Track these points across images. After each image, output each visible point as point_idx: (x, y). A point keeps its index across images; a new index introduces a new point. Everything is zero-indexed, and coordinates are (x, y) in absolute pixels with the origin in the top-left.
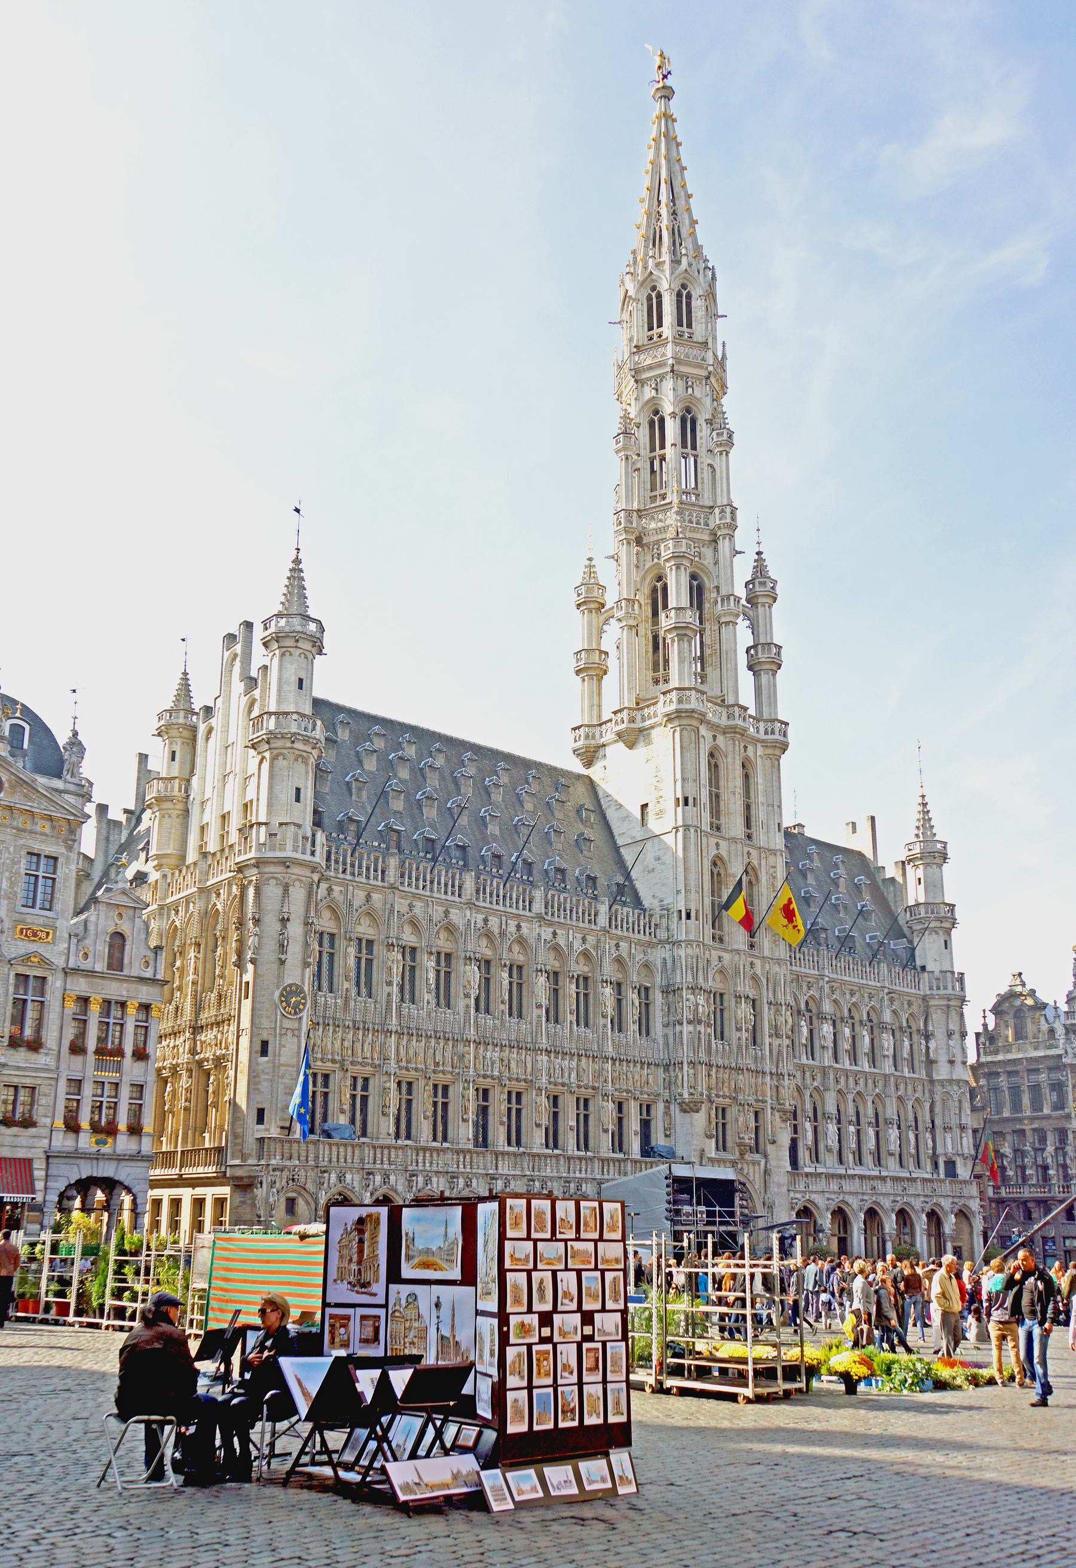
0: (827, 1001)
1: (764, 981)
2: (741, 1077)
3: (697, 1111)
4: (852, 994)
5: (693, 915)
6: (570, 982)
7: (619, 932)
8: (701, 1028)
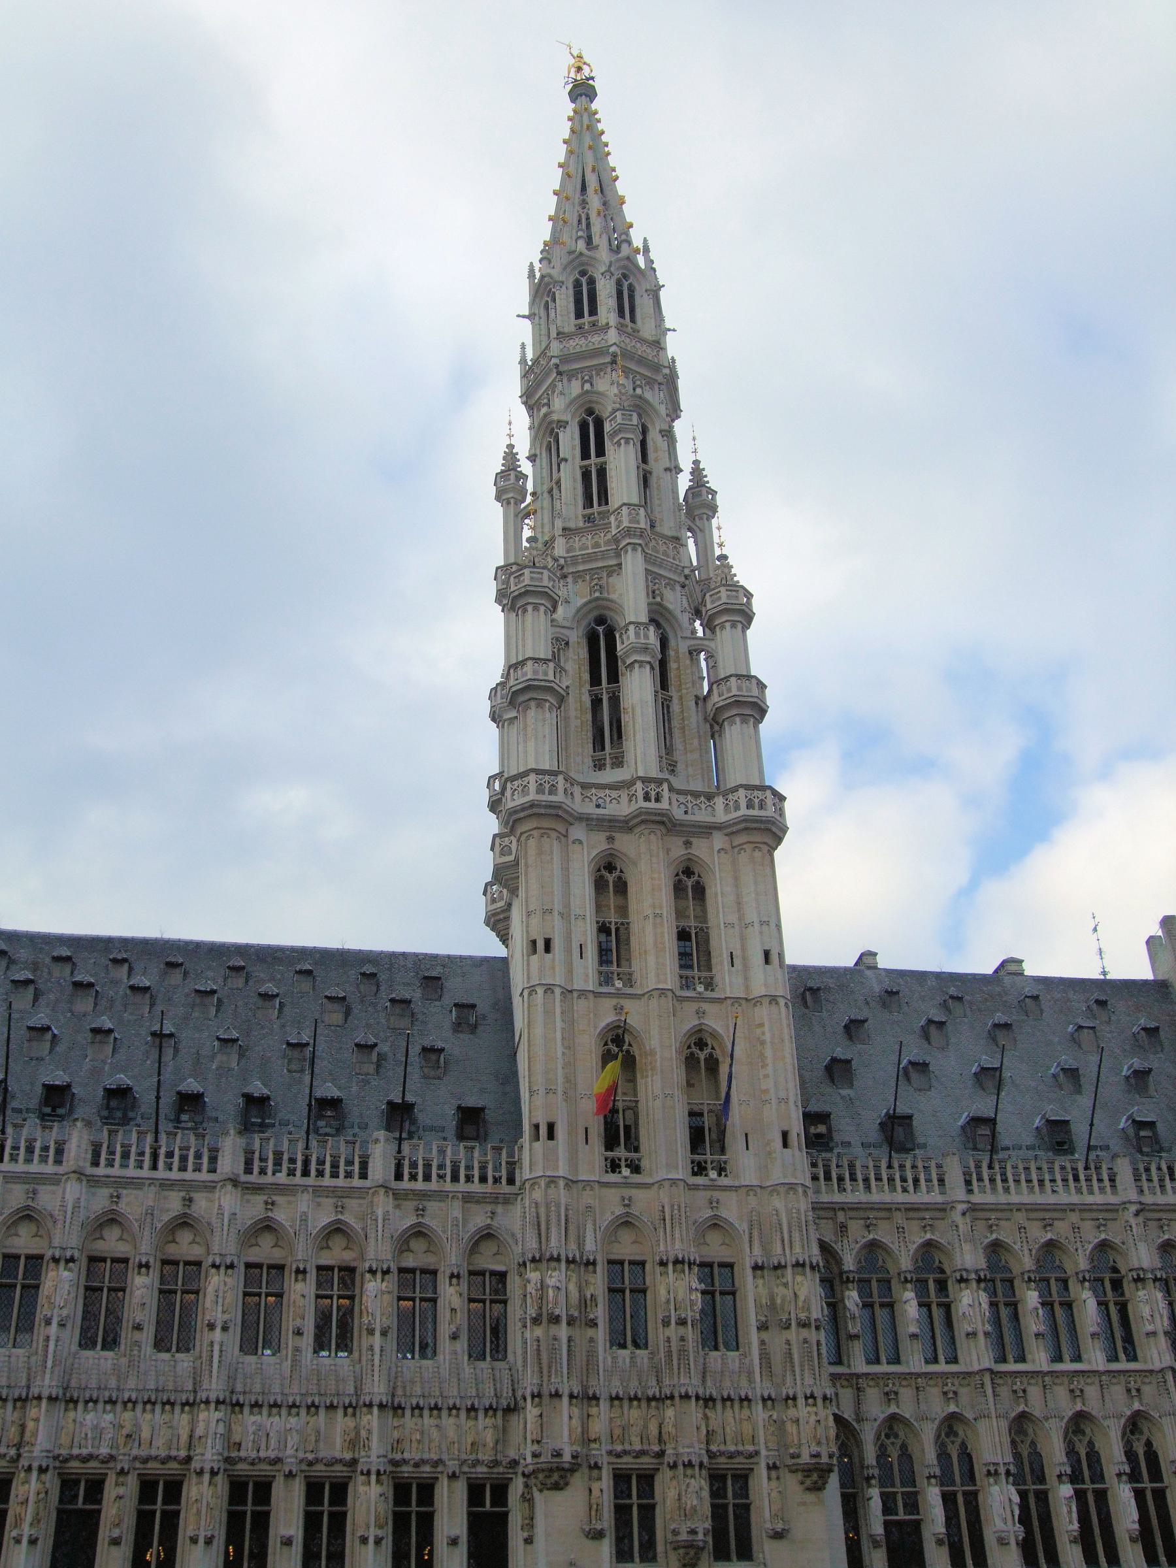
0: (967, 1247)
1: (742, 1227)
2: (670, 1413)
3: (557, 1487)
4: (1047, 1226)
5: (543, 1131)
6: (296, 1280)
7: (420, 1185)
8: (563, 1331)
